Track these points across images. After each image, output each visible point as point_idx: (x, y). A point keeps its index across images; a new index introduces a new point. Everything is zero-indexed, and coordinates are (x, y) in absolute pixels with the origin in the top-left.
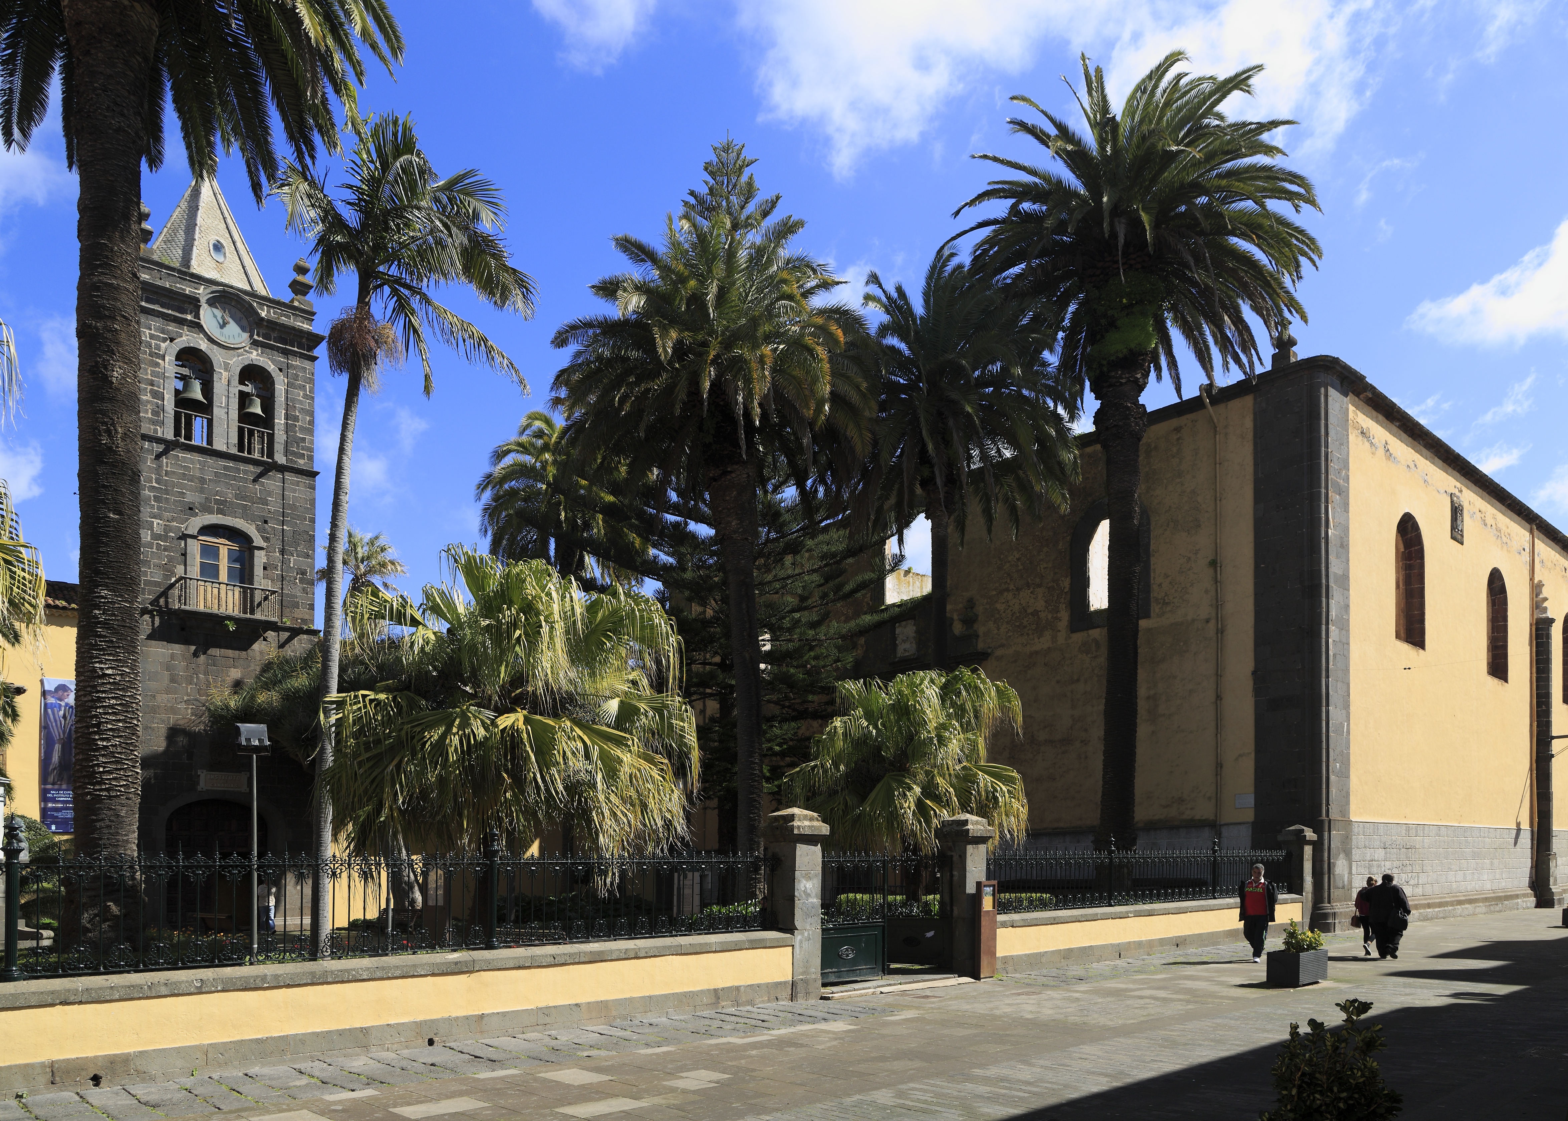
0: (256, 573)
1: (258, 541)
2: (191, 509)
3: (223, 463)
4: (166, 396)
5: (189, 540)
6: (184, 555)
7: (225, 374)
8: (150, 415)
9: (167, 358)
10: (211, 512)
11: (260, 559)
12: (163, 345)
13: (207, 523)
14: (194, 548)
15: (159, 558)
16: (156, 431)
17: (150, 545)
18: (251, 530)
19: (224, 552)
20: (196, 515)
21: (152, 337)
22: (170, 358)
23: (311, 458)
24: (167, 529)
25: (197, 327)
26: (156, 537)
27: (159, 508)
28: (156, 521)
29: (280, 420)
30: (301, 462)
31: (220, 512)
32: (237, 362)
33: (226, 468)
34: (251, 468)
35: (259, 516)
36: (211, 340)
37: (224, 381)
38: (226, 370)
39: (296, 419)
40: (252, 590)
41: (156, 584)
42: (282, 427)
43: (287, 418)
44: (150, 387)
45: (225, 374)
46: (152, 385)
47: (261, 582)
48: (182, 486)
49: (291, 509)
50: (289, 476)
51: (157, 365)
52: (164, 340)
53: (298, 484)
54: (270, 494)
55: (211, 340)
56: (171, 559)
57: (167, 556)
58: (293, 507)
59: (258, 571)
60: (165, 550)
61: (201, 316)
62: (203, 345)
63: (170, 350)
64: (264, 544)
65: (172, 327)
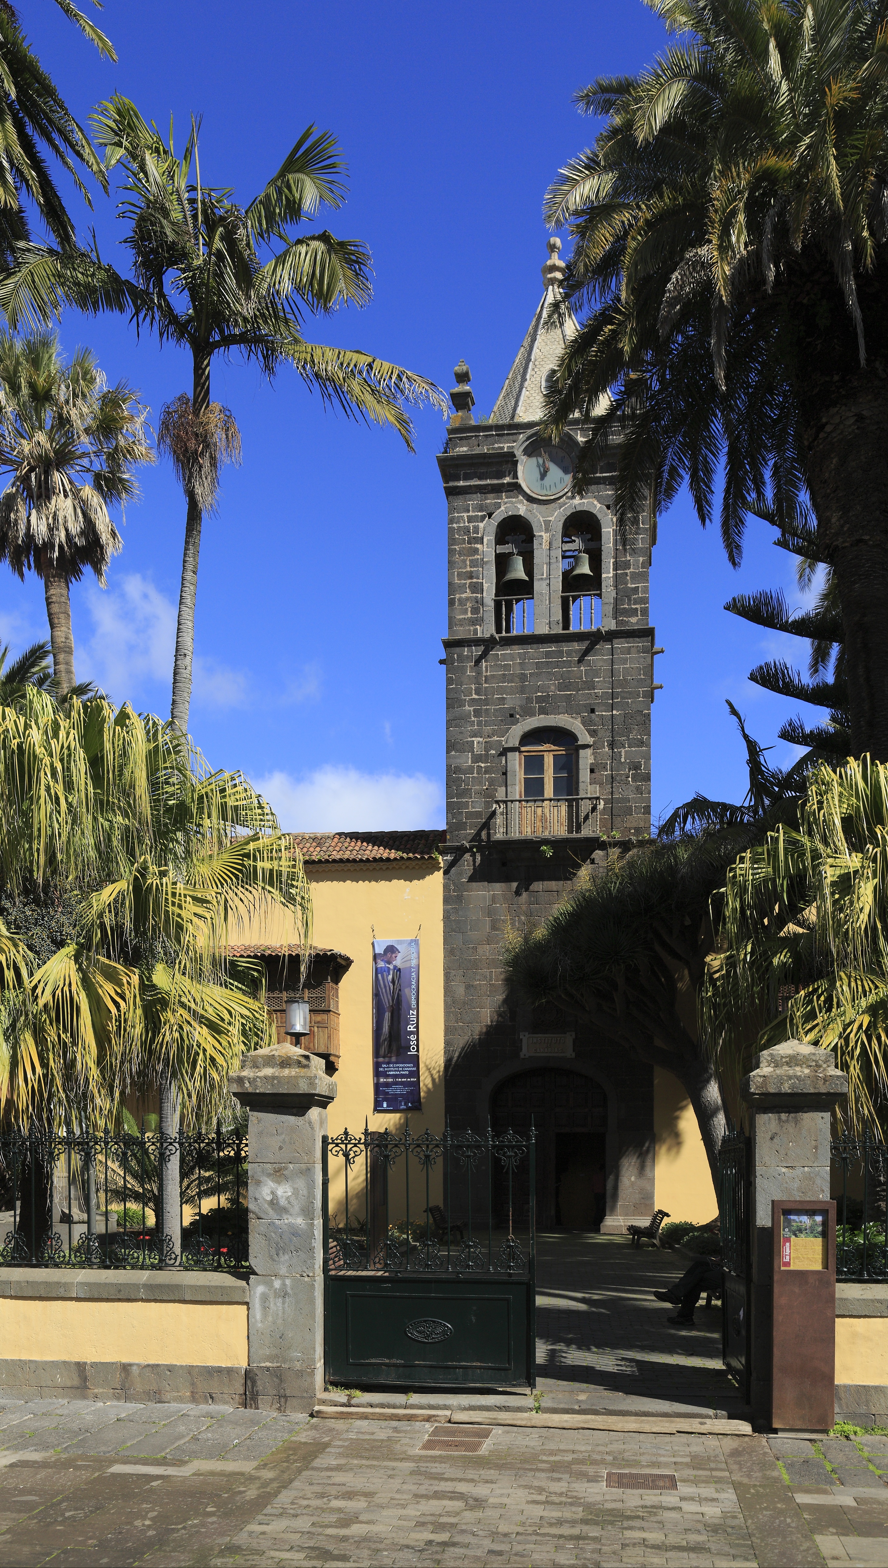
0: (581, 779)
1: (584, 738)
2: (512, 716)
3: (544, 649)
4: (485, 586)
5: (509, 754)
6: (505, 774)
7: (546, 536)
8: (469, 615)
9: (485, 540)
10: (532, 715)
11: (586, 758)
12: (481, 525)
13: (527, 728)
14: (516, 762)
15: (480, 783)
16: (476, 631)
17: (470, 770)
18: (574, 724)
19: (549, 761)
20: (517, 721)
21: (470, 519)
22: (489, 538)
23: (645, 612)
24: (488, 746)
25: (515, 488)
26: (477, 759)
27: (479, 723)
28: (476, 740)
29: (608, 574)
30: (634, 620)
31: (543, 711)
32: (557, 516)
33: (548, 655)
34: (576, 646)
35: (585, 706)
36: (531, 499)
37: (545, 546)
38: (547, 530)
39: (627, 565)
40: (577, 800)
41: (478, 815)
42: (611, 582)
43: (616, 569)
44: (468, 581)
45: (546, 536)
46: (471, 577)
47: (587, 787)
48: (501, 690)
49: (621, 686)
50: (620, 644)
51: (476, 551)
52: (482, 519)
53: (628, 651)
54: (597, 674)
55: (531, 499)
56: (492, 782)
57: (488, 780)
58: (624, 683)
59: (584, 775)
60: (486, 772)
61: (520, 474)
62: (522, 508)
63: (488, 529)
64: (590, 740)
65: (490, 500)
